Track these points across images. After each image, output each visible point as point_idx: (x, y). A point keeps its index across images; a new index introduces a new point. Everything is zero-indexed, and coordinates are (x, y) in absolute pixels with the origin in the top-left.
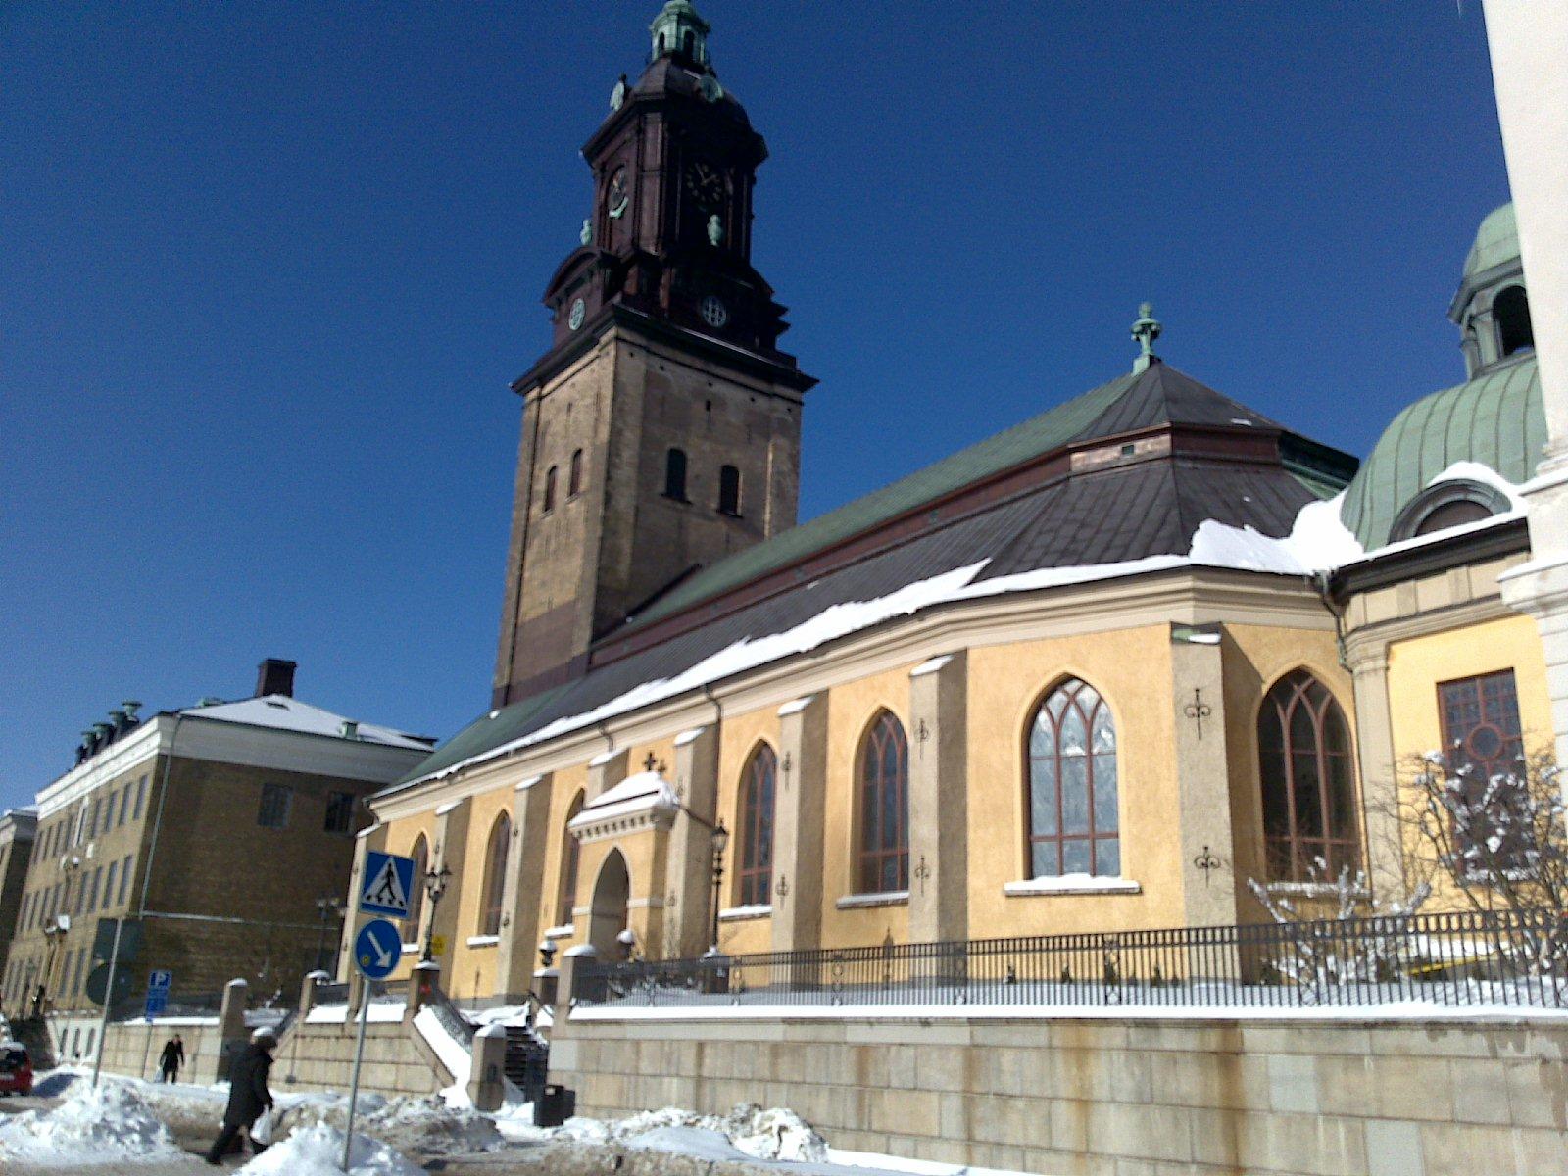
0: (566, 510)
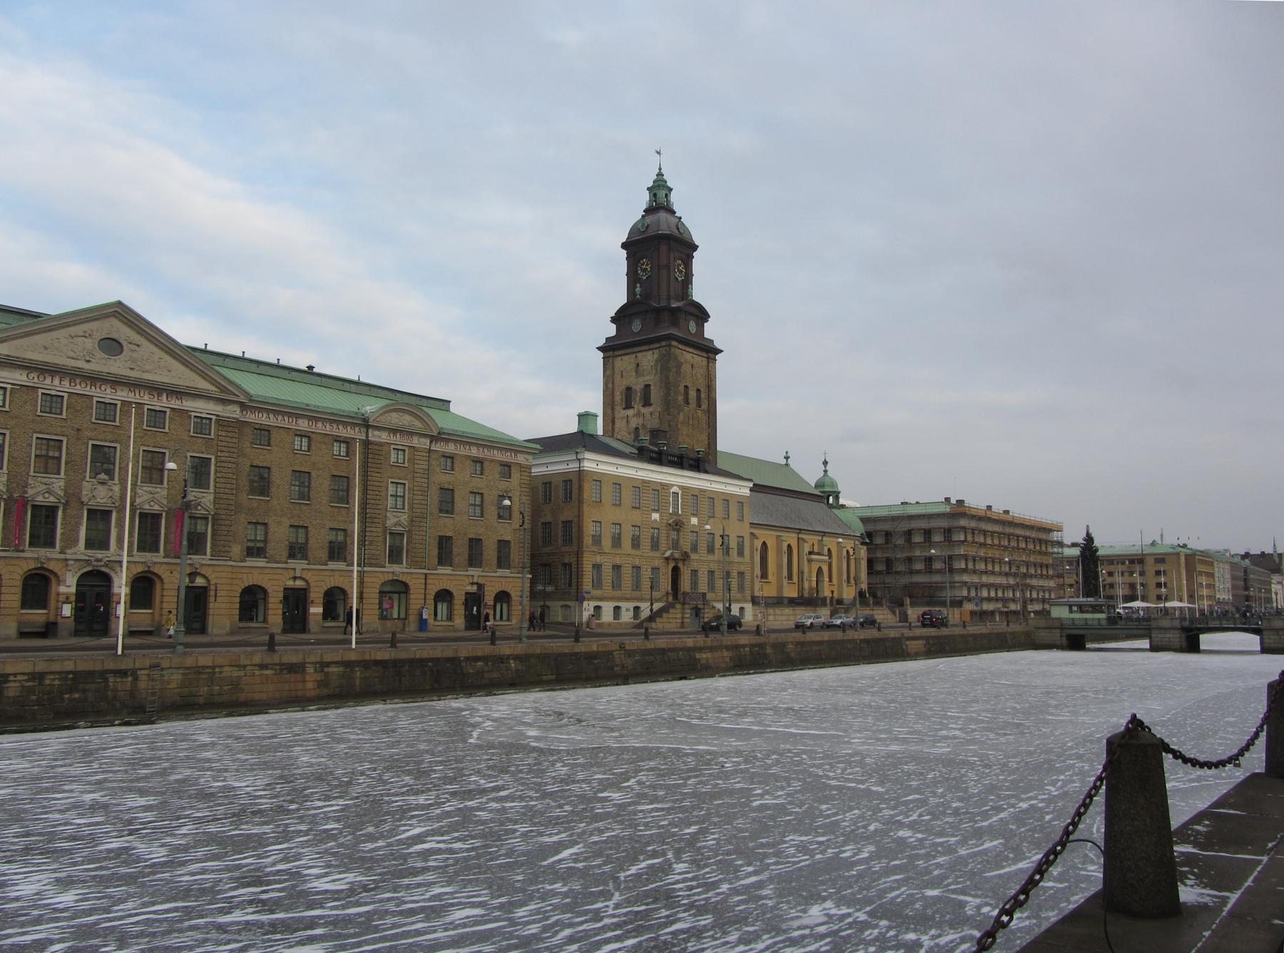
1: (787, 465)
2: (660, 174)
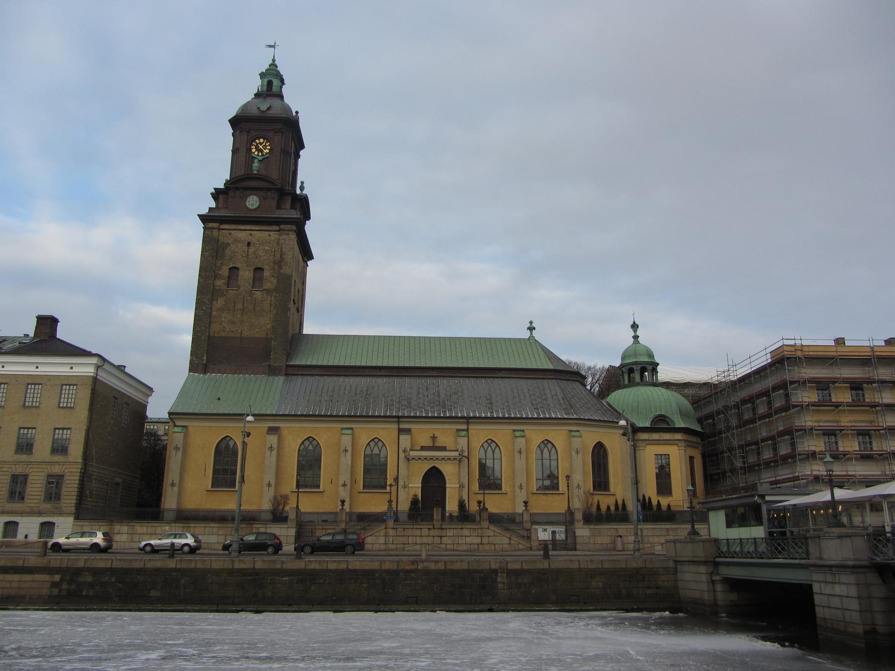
0: (251, 293)
1: (531, 337)
2: (273, 65)
